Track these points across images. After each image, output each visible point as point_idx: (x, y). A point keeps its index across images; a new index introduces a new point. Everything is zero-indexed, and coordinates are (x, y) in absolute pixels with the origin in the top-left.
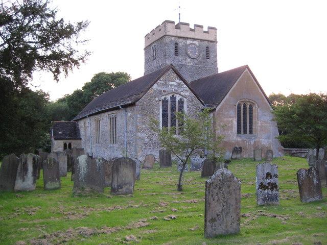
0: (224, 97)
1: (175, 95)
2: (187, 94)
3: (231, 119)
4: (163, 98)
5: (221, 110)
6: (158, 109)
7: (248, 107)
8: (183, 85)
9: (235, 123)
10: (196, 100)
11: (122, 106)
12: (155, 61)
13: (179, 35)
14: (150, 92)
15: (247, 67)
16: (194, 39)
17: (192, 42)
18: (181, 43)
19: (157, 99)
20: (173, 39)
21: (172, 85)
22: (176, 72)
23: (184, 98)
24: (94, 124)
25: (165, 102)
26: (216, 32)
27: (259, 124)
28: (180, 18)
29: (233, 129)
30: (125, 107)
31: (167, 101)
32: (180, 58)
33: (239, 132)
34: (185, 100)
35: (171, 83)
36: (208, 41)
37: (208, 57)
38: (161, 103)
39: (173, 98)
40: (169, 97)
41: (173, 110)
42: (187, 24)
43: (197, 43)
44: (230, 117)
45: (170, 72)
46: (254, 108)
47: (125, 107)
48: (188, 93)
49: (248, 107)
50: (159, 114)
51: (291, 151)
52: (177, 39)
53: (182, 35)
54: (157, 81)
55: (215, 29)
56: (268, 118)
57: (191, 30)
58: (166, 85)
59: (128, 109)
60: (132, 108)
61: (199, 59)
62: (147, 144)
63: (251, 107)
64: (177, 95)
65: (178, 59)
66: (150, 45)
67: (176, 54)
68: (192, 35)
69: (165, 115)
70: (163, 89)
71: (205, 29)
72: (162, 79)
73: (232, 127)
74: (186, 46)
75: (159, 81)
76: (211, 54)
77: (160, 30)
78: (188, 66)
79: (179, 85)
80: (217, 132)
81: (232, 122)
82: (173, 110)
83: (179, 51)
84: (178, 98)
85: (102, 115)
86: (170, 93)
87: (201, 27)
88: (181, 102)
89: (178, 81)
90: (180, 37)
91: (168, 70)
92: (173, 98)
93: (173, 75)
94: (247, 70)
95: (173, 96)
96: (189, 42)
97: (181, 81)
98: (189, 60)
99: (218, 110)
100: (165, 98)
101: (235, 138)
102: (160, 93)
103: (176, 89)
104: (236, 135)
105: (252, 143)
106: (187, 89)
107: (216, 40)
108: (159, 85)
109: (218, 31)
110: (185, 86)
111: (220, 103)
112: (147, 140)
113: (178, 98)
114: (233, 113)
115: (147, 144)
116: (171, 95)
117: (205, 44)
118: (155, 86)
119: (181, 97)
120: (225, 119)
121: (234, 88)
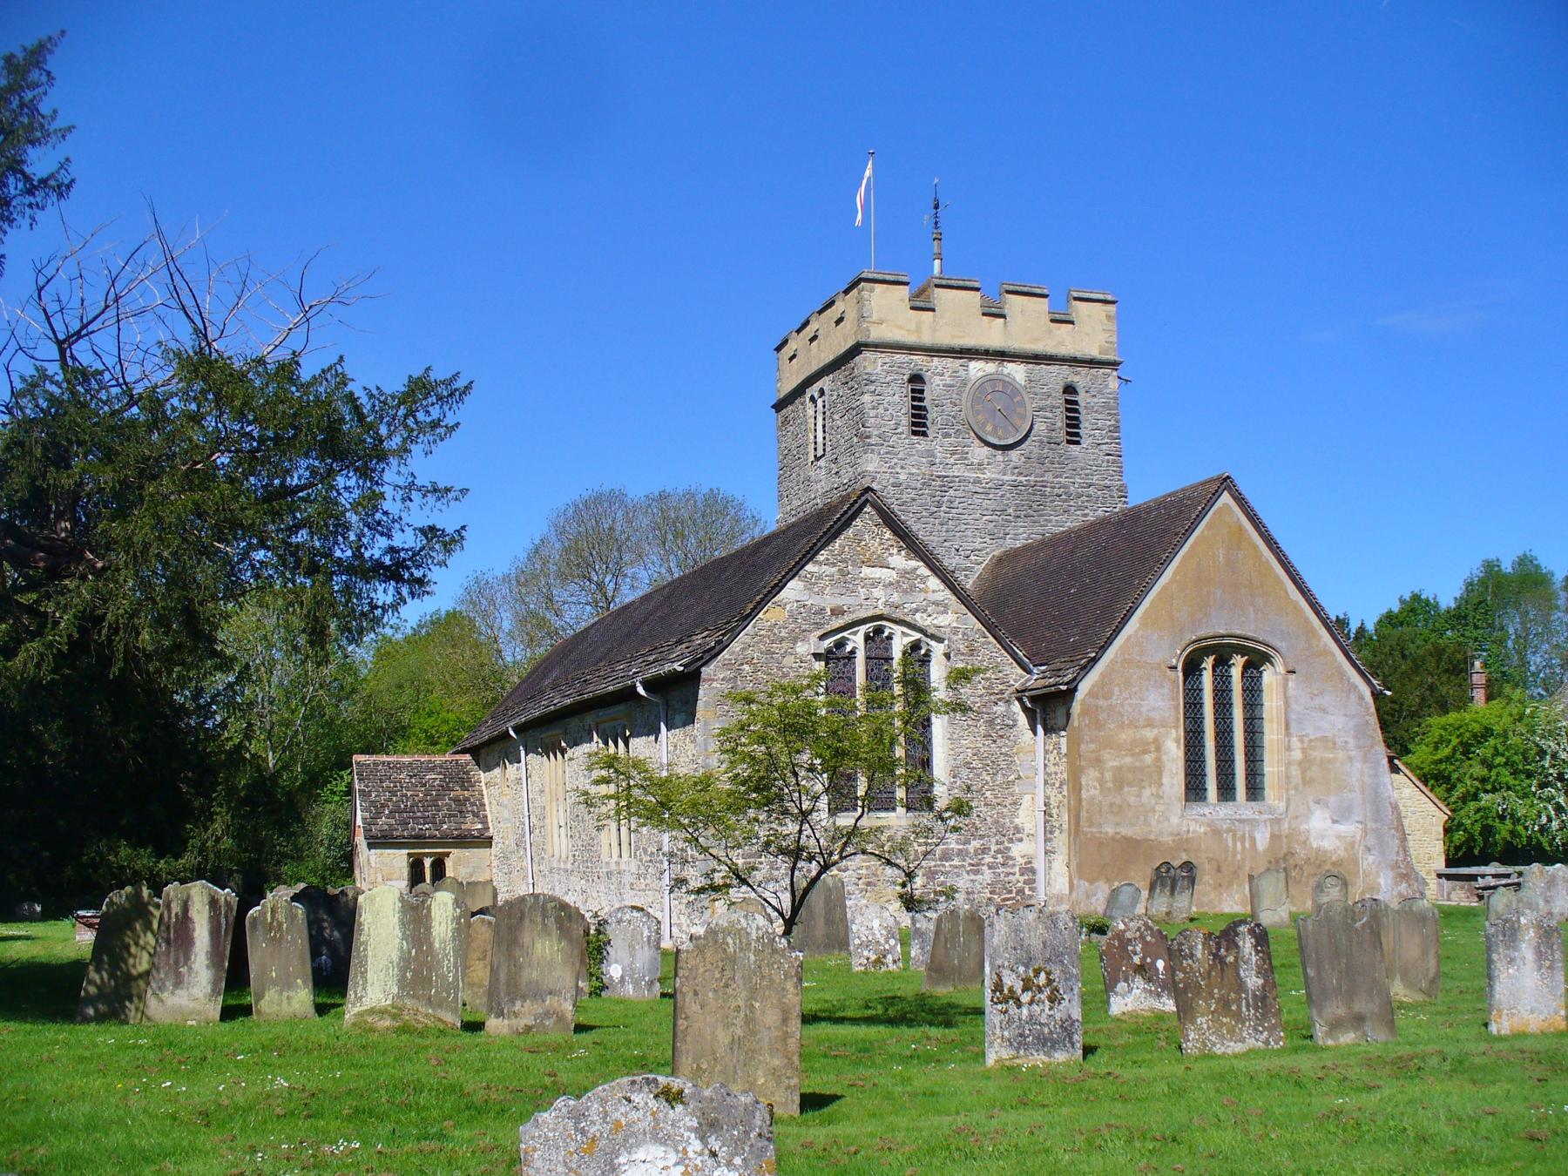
0: (1117, 631)
1: (889, 627)
2: (946, 620)
3: (1149, 734)
8: (924, 579)
9: (1174, 751)
12: (822, 463)
13: (927, 339)
14: (770, 616)
16: (1001, 355)
17: (991, 367)
18: (940, 373)
21: (875, 583)
22: (889, 520)
23: (933, 643)
27: (1297, 755)
29: (1165, 780)
32: (936, 443)
33: (1194, 790)
34: (938, 649)
35: (867, 571)
36: (1074, 361)
40: (856, 640)
43: (1017, 372)
44: (1150, 723)
48: (951, 618)
51: (1473, 878)
53: (946, 339)
54: (800, 565)
56: (1340, 721)
58: (845, 581)
64: (899, 629)
65: (930, 454)
67: (918, 423)
68: (992, 335)
70: (829, 602)
73: (1159, 767)
75: (810, 567)
78: (977, 481)
79: (906, 581)
80: (1084, 794)
81: (1158, 749)
84: (900, 642)
85: (574, 722)
88: (917, 656)
89: (900, 560)
94: (1226, 498)
95: (879, 631)
97: (914, 563)
100: (840, 644)
101: (1175, 820)
103: (896, 598)
104: (1178, 805)
105: (1262, 838)
108: (809, 585)
110: (934, 583)
111: (1094, 660)
113: (900, 642)
114: (1162, 702)
118: (793, 590)
120: (1125, 736)
121: (1164, 588)
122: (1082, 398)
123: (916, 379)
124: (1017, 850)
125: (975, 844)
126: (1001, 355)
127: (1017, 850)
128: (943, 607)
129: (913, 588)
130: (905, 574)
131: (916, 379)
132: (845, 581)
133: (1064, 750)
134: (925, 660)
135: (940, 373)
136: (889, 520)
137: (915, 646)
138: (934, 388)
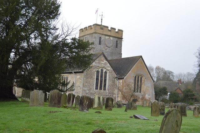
1: (103, 69)
2: (109, 68)
4: (97, 70)
5: (126, 78)
6: (94, 76)
7: (140, 78)
10: (113, 73)
11: (74, 72)
13: (102, 33)
15: (141, 57)
16: (110, 36)
17: (109, 37)
18: (103, 37)
19: (94, 70)
20: (99, 35)
22: (105, 56)
23: (108, 71)
25: (98, 72)
26: (122, 33)
27: (145, 88)
28: (102, 22)
30: (75, 73)
31: (99, 72)
32: (102, 46)
34: (108, 72)
37: (117, 47)
38: (96, 72)
39: (102, 70)
40: (100, 70)
41: (102, 77)
42: (107, 27)
43: (111, 38)
45: (102, 56)
46: (143, 79)
48: (110, 68)
49: (140, 78)
50: (94, 78)
52: (101, 35)
55: (122, 31)
57: (110, 31)
58: (99, 63)
59: (78, 74)
60: (81, 74)
61: (112, 48)
62: (87, 94)
63: (141, 78)
67: (100, 44)
68: (109, 33)
69: (97, 79)
72: (97, 59)
76: (119, 45)
77: (91, 28)
79: (105, 64)
82: (102, 77)
83: (102, 42)
86: (101, 68)
87: (115, 29)
88: (106, 73)
89: (105, 61)
90: (102, 34)
91: (100, 55)
92: (102, 70)
93: (103, 58)
94: (141, 58)
96: (107, 37)
97: (106, 62)
99: (125, 79)
100: (98, 70)
102: (96, 67)
103: (104, 65)
106: (109, 66)
107: (122, 36)
110: (108, 64)
112: (87, 92)
115: (87, 94)
116: (101, 69)
119: (106, 70)
122: (118, 42)
123: (100, 38)
124: (114, 96)
125: (110, 95)
126: (110, 36)
127: (114, 96)
128: (109, 67)
129: (106, 65)
130: (105, 63)
131: (100, 38)
132: (99, 63)
133: (121, 85)
134: (107, 73)
135: (103, 37)
136: (105, 56)
137: (106, 71)
138: (102, 39)
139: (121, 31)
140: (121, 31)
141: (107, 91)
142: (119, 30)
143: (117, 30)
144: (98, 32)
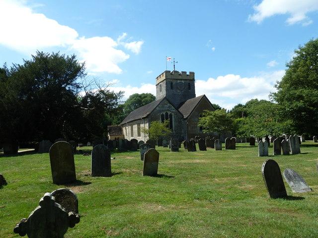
20: (170, 80)
24: (130, 127)
34: (173, 114)
43: (183, 82)
47: (144, 118)
66: (158, 84)
67: (172, 88)
68: (180, 77)
71: (188, 73)
74: (177, 83)
79: (169, 107)
87: (185, 73)
90: (174, 79)
96: (178, 81)
98: (179, 91)
102: (160, 111)
109: (195, 74)
113: (169, 113)
117: (188, 81)
127: (182, 135)
134: (172, 115)
138: (174, 83)
139: (192, 74)
140: (192, 74)
141: (174, 132)
142: (190, 73)
143: (188, 73)
144: (169, 77)
